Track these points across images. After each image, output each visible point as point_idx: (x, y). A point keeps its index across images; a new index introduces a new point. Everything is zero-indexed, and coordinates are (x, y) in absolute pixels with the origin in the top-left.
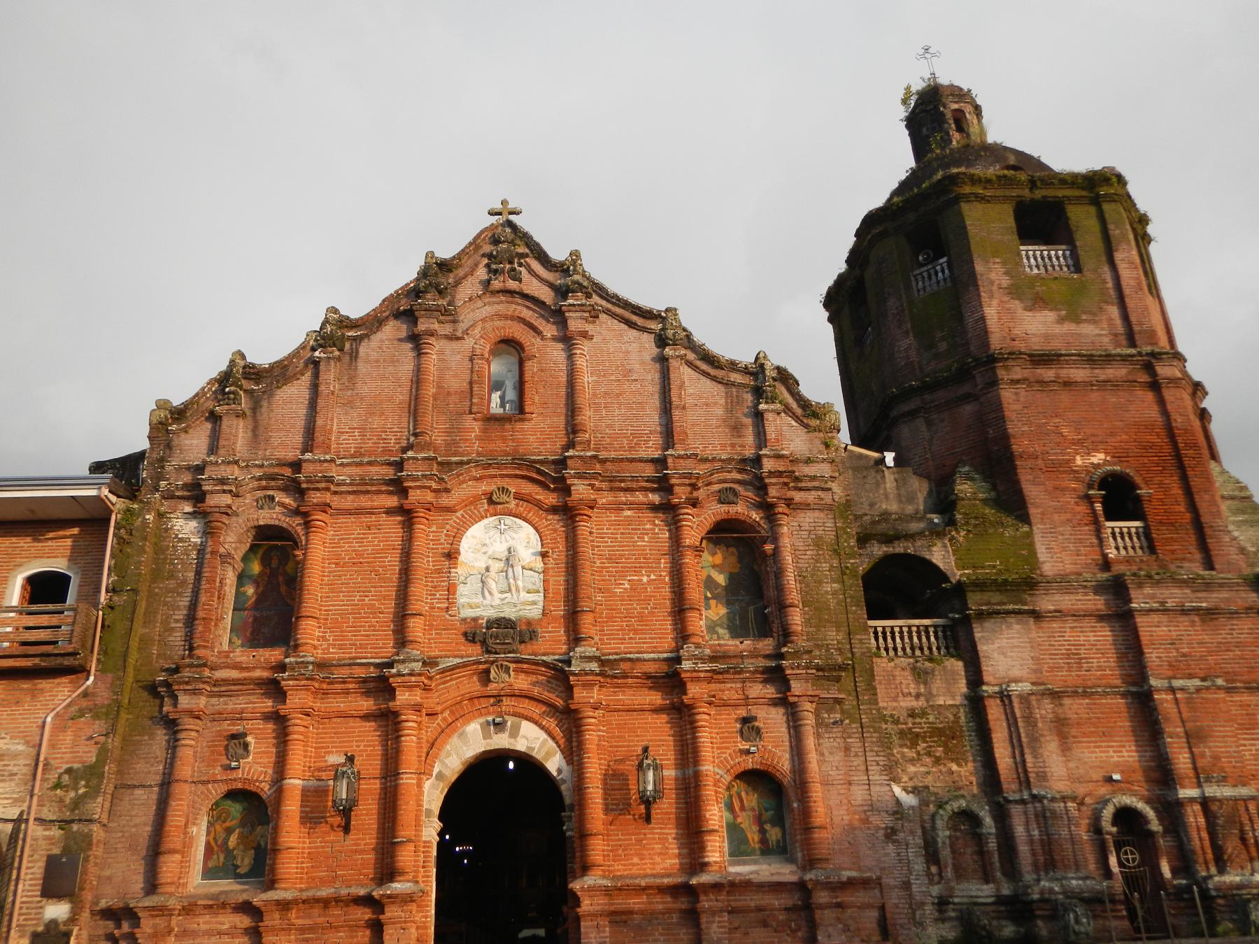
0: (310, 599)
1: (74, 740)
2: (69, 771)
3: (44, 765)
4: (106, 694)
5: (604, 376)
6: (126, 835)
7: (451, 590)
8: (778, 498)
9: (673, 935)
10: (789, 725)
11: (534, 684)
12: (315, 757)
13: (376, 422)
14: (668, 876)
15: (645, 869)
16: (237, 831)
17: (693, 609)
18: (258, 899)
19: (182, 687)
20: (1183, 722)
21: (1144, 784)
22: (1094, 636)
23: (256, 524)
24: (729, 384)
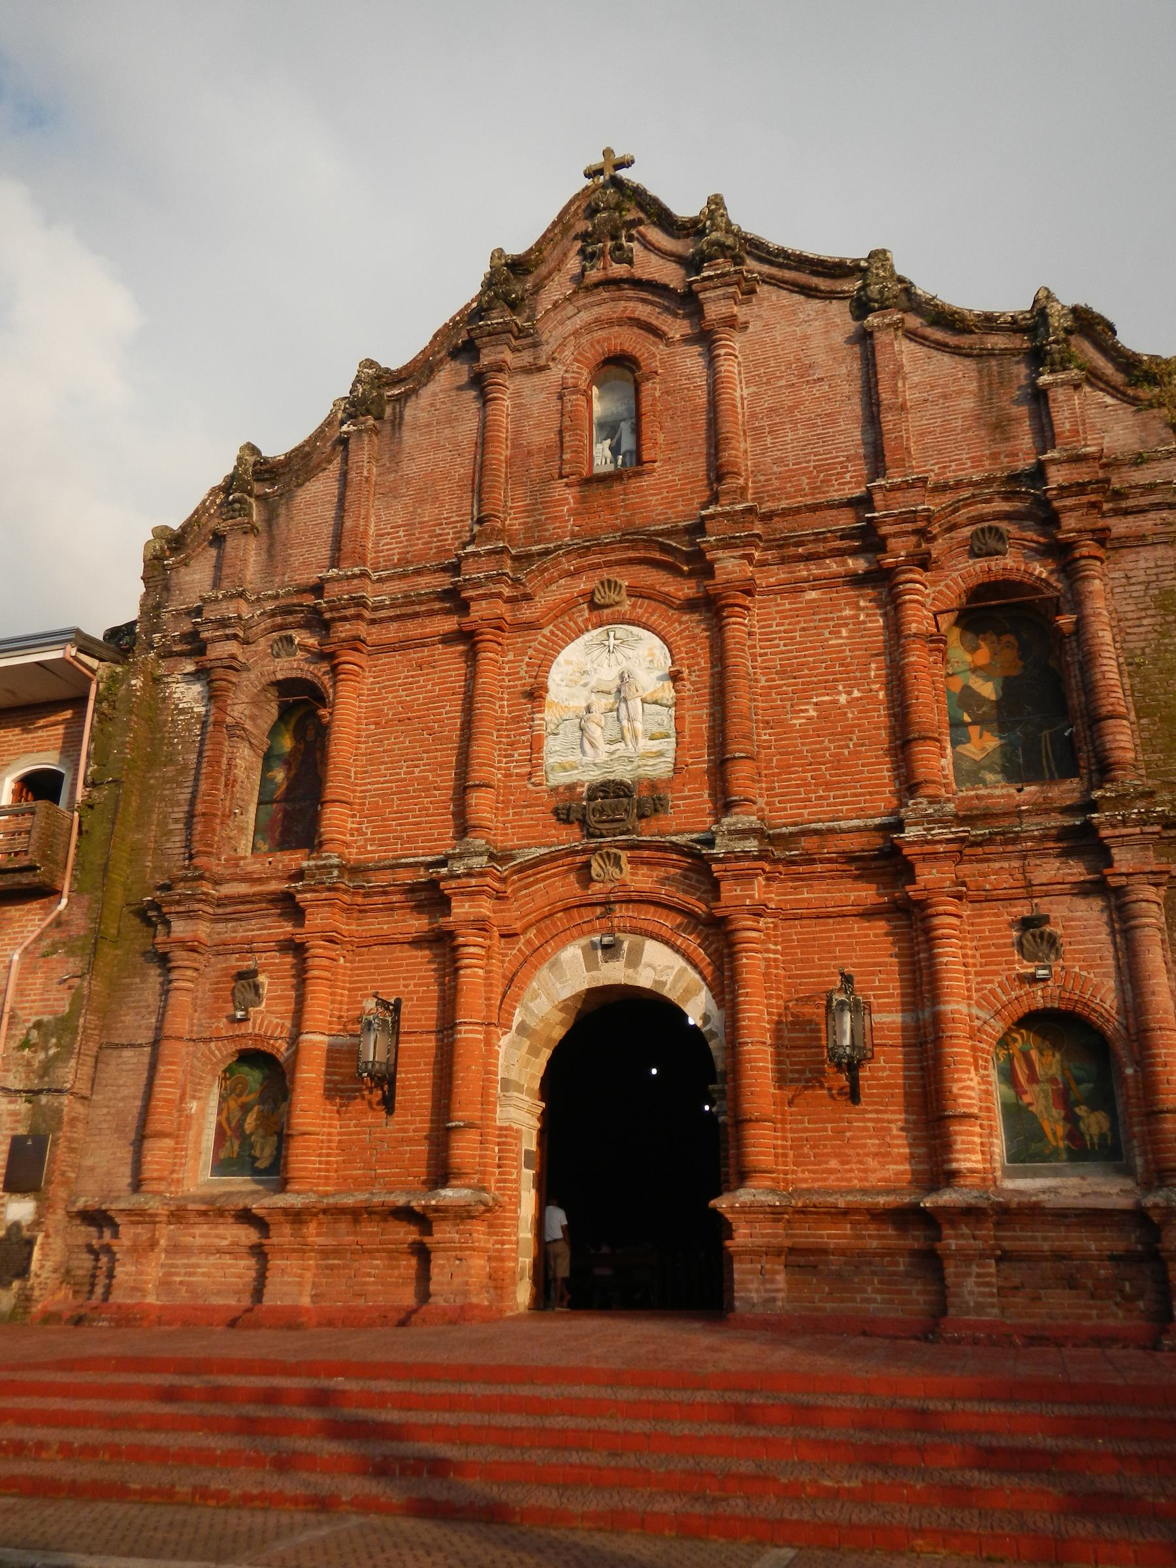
0: (337, 775)
1: (45, 984)
2: (38, 1025)
3: (11, 1017)
4: (82, 922)
5: (768, 382)
6: (113, 1111)
7: (536, 745)
8: (1079, 531)
9: (899, 1292)
10: (1112, 927)
11: (662, 881)
12: (348, 1004)
13: (428, 513)
14: (889, 1191)
15: (849, 1180)
16: (256, 1108)
17: (925, 738)
18: (265, 1203)
19: (173, 909)
23: (273, 678)
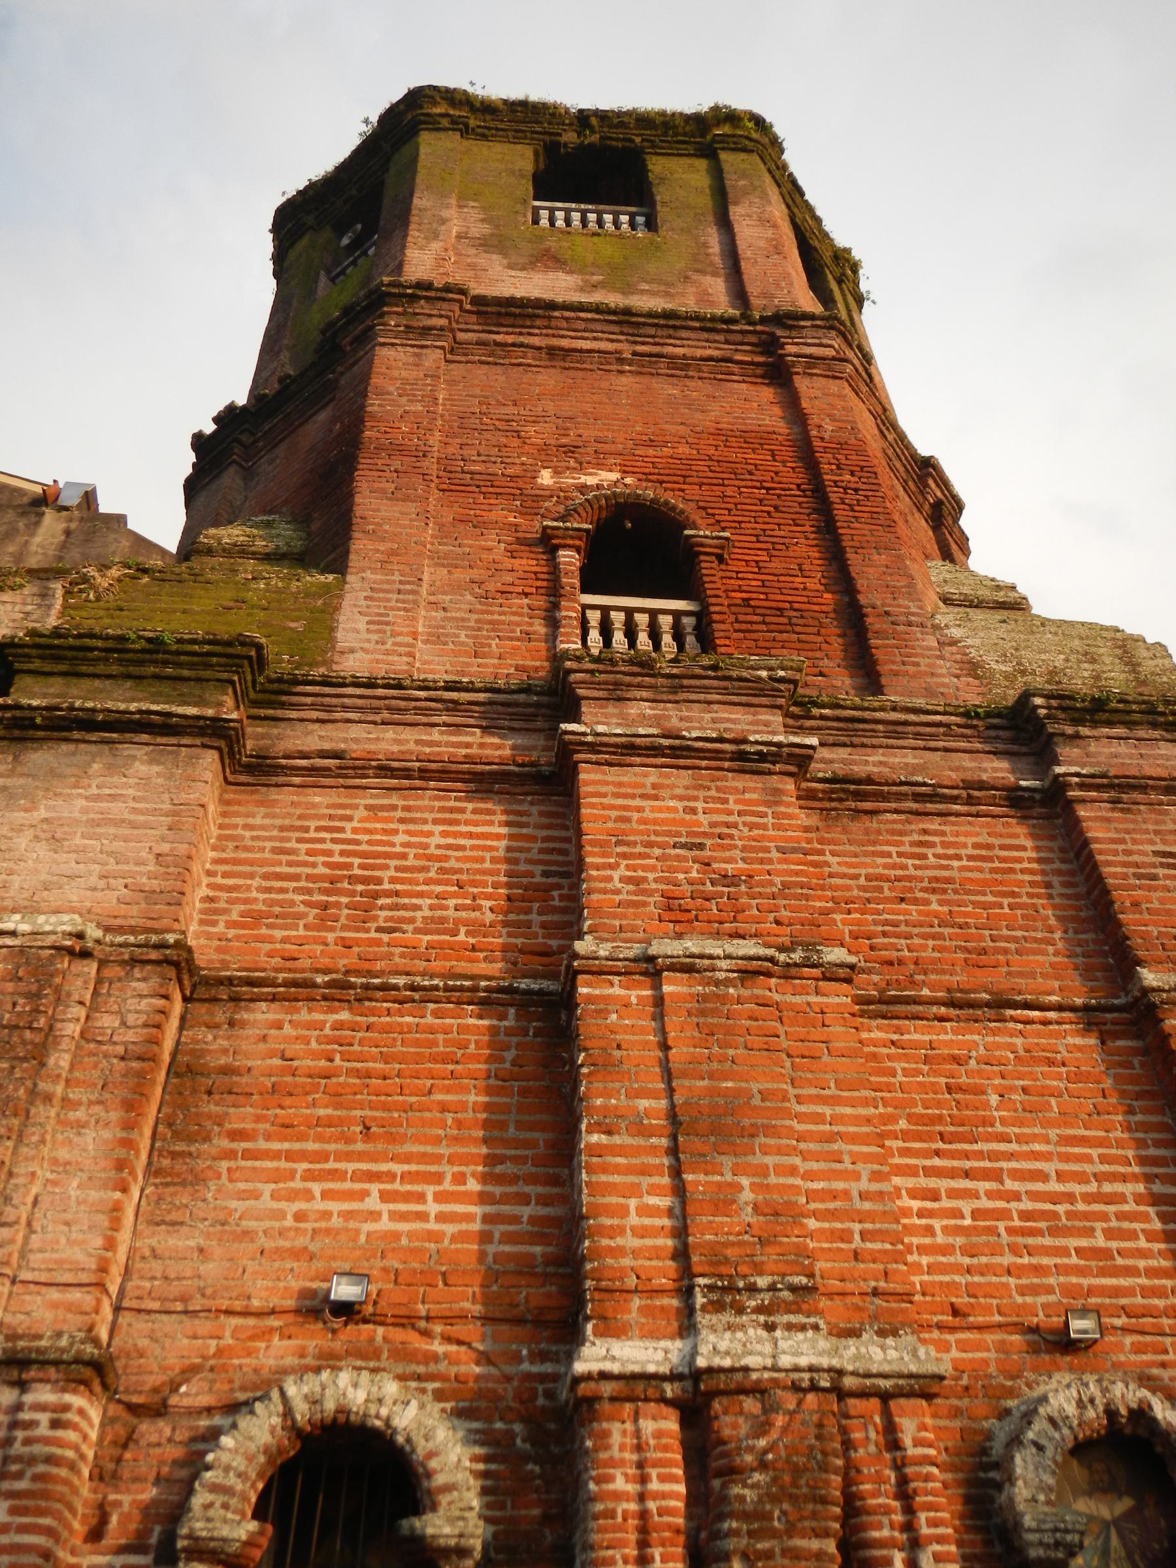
20: (668, 1075)
21: (470, 1331)
22: (444, 834)
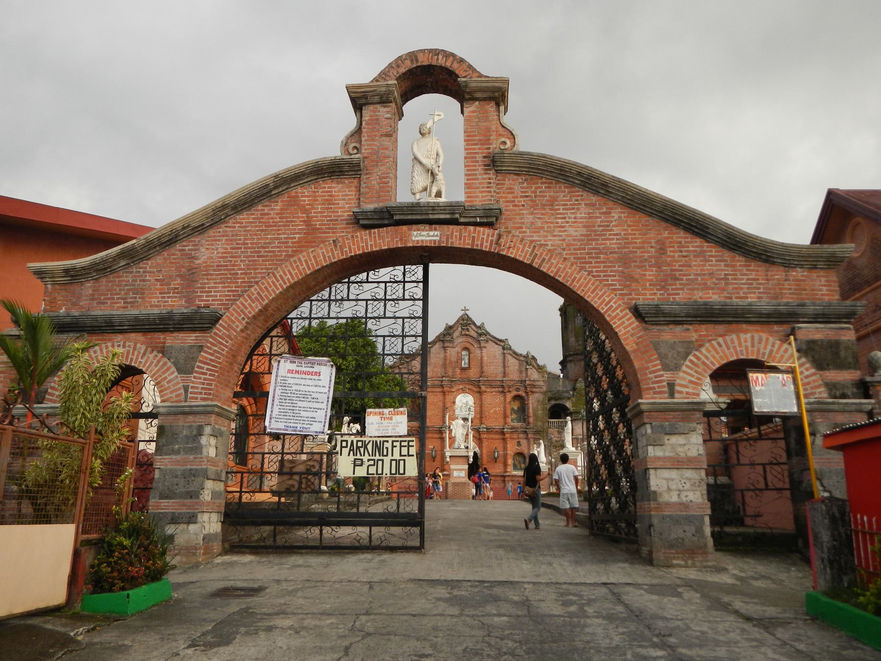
7: (454, 411)
24: (520, 360)
